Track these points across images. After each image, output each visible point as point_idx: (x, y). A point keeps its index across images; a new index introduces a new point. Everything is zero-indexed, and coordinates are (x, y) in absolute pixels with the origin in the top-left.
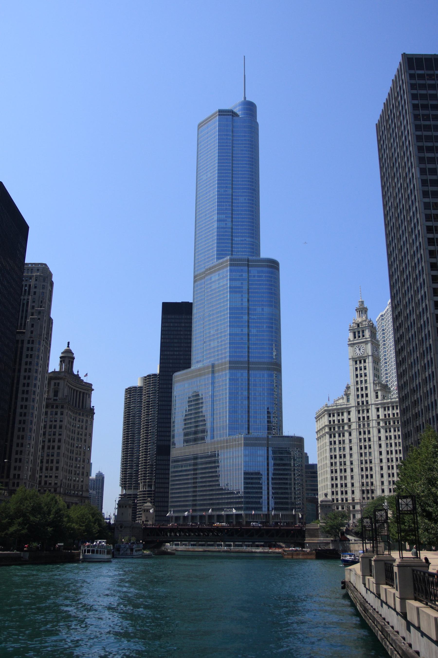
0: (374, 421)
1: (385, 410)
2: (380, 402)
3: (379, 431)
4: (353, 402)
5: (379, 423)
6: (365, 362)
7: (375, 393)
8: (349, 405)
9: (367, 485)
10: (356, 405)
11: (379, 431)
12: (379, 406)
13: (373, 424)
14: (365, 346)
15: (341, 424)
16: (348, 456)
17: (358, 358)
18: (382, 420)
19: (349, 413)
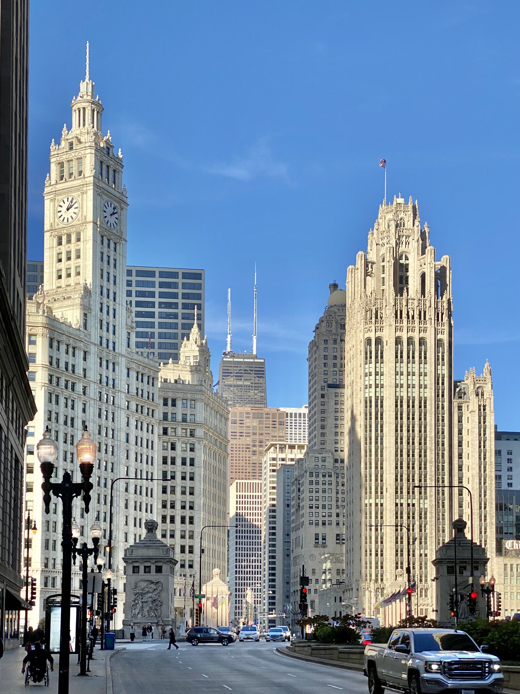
0: (123, 396)
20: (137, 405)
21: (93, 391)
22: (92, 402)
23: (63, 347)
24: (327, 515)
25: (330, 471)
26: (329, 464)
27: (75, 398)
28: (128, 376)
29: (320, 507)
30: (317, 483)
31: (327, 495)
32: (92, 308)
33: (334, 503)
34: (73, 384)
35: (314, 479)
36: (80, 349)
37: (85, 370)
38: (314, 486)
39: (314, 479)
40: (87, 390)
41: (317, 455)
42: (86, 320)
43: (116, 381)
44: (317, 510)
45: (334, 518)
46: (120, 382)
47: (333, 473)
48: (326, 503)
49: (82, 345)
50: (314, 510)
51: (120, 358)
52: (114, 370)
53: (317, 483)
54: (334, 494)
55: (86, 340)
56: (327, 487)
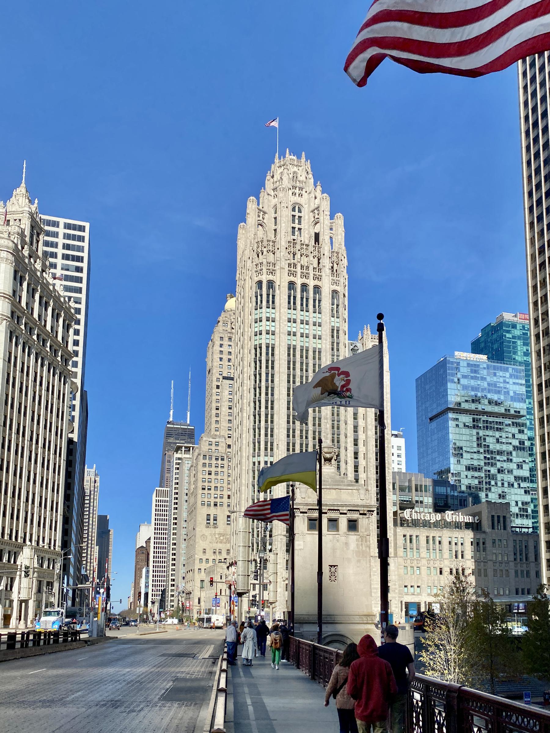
24: (219, 497)
25: (223, 455)
26: (222, 448)
29: (213, 488)
30: (210, 465)
31: (219, 477)
33: (225, 485)
35: (207, 461)
38: (207, 469)
39: (207, 461)
41: (211, 440)
44: (209, 492)
45: (225, 500)
47: (225, 457)
48: (219, 485)
50: (206, 491)
53: (210, 465)
54: (225, 477)
56: (219, 469)
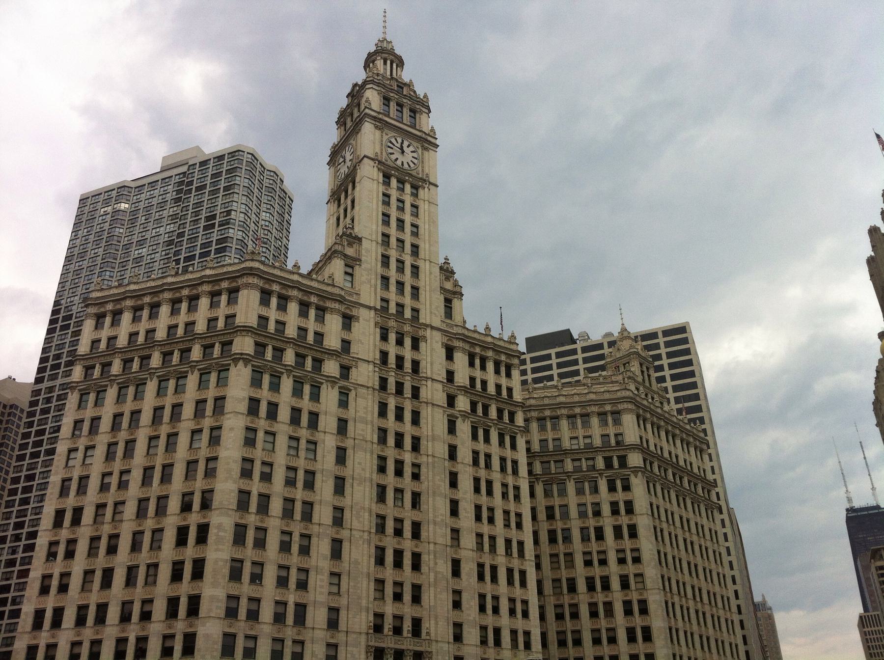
0: (439, 386)
1: (472, 364)
2: (455, 330)
3: (452, 429)
4: (368, 290)
5: (451, 401)
6: (415, 195)
7: (442, 298)
8: (351, 294)
9: (398, 631)
10: (379, 308)
11: (452, 429)
12: (456, 343)
13: (433, 392)
14: (420, 151)
15: (313, 351)
16: (325, 488)
17: (397, 169)
18: (463, 389)
19: (348, 320)
20: (474, 405)
21: (365, 375)
22: (362, 391)
23: (293, 307)
27: (322, 383)
28: (450, 357)
32: (363, 258)
34: (318, 363)
36: (332, 311)
37: (346, 344)
40: (353, 373)
42: (351, 275)
43: (422, 365)
46: (429, 366)
49: (337, 306)
51: (429, 330)
52: (415, 346)
55: (346, 300)
